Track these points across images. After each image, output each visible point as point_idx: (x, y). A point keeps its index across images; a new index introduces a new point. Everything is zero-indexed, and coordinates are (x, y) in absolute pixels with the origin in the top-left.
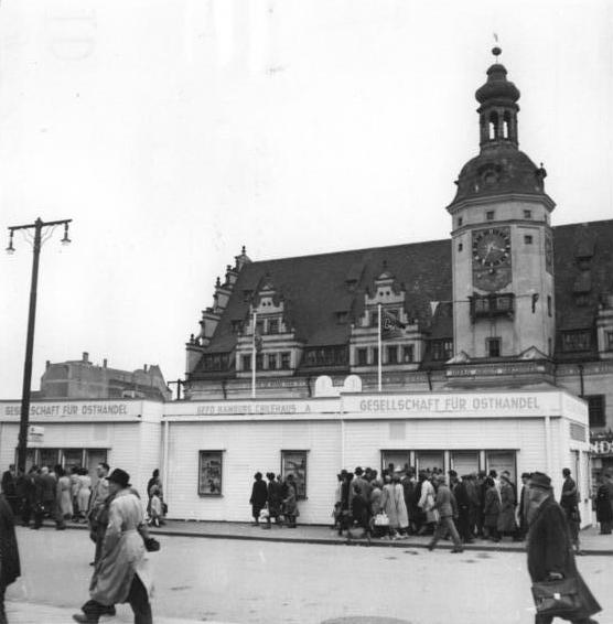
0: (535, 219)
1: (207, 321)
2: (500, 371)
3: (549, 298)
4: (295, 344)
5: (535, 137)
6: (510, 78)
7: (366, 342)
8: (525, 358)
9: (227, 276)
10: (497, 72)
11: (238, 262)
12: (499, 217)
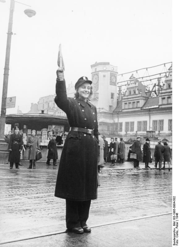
3: (112, 95)
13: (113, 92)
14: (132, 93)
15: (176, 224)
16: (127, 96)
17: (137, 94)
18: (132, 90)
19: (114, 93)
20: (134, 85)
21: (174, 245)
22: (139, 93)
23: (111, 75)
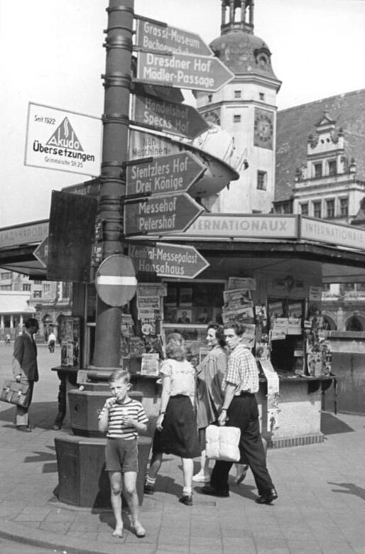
7: (333, 192)
13: (262, 169)
14: (326, 170)
16: (312, 179)
17: (341, 175)
18: (324, 162)
20: (332, 147)
22: (348, 172)
23: (256, 114)
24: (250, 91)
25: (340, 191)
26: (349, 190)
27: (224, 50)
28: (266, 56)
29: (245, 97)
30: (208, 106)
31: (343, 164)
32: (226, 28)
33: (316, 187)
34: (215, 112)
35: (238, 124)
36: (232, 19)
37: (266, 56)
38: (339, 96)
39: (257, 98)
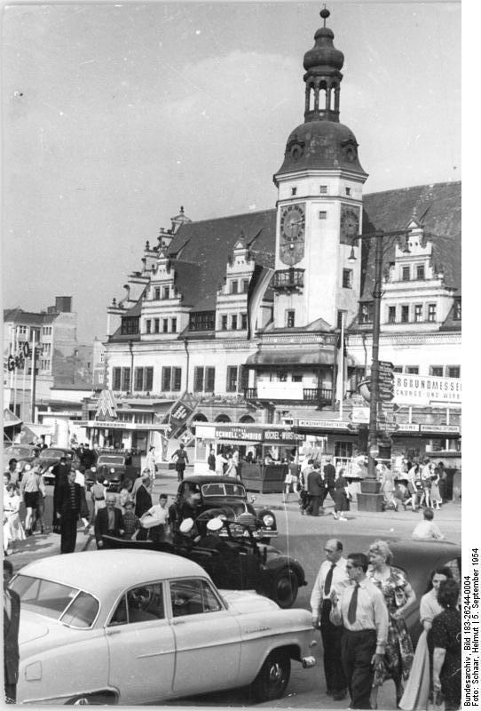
0: (332, 195)
1: (130, 285)
2: (292, 341)
3: (347, 273)
4: (180, 309)
5: (356, 105)
6: (338, 44)
8: (309, 330)
9: (160, 239)
10: (324, 36)
11: (174, 225)
12: (299, 194)
14: (413, 273)
15: (472, 645)
17: (429, 280)
19: (351, 270)
21: (467, 704)
23: (342, 210)
24: (335, 185)
25: (428, 296)
26: (436, 296)
27: (309, 142)
28: (352, 147)
29: (333, 191)
30: (292, 199)
31: (431, 269)
32: (311, 115)
33: (404, 290)
34: (301, 206)
35: (323, 220)
36: (316, 106)
37: (352, 147)
38: (428, 187)
39: (344, 194)
